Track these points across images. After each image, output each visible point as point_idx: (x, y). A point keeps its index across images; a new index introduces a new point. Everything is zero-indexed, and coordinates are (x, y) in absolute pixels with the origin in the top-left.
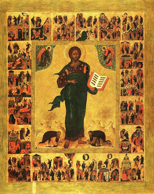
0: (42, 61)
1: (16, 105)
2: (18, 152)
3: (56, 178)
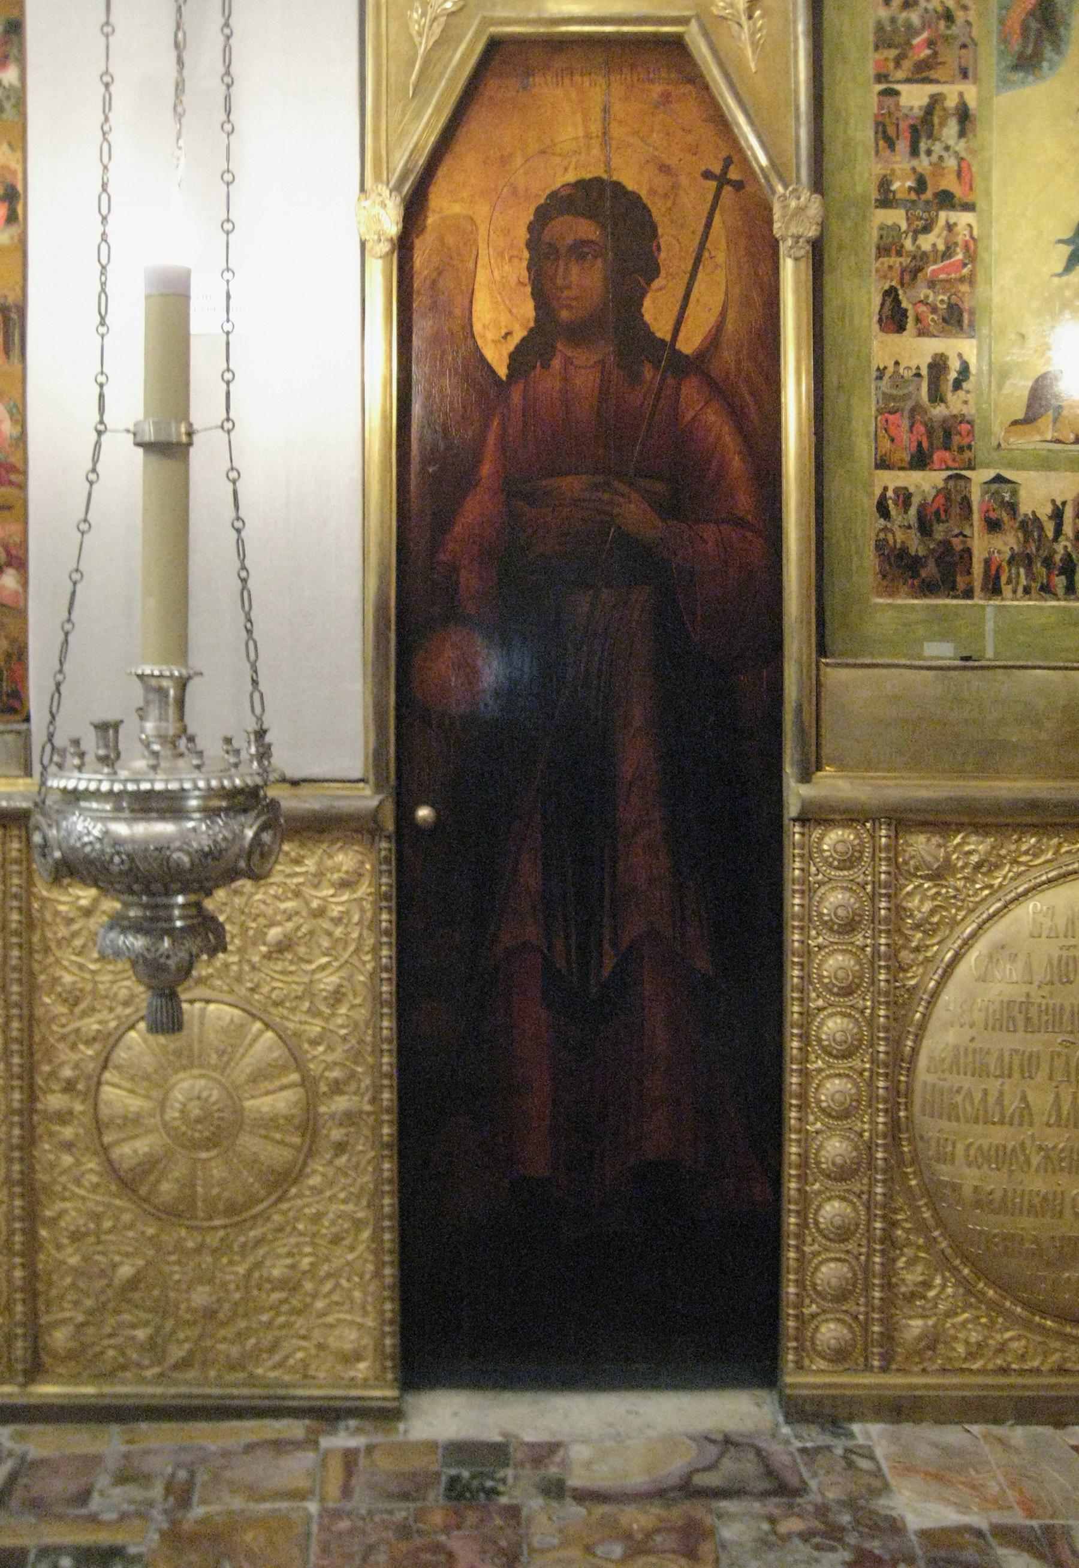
1: (908, 244)
2: (920, 461)
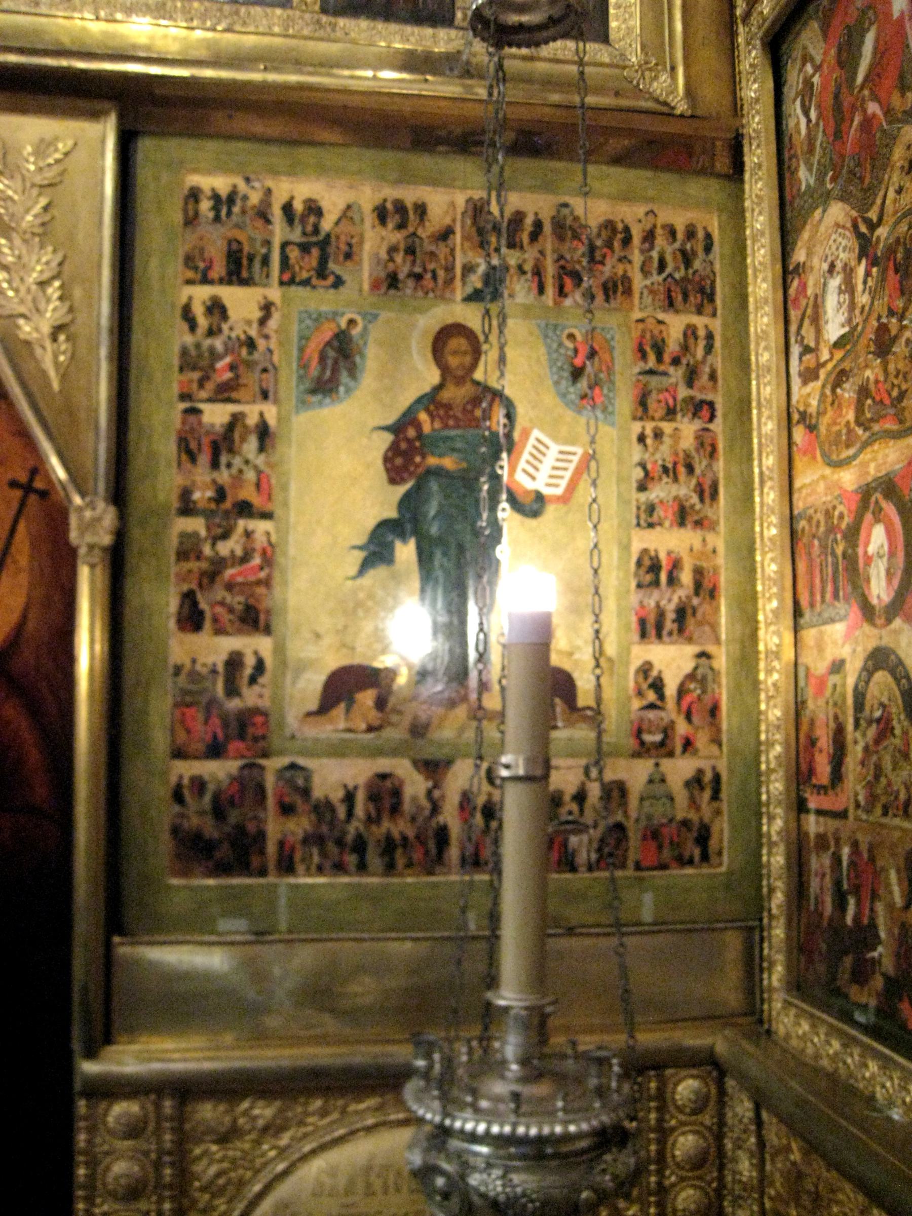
0: (323, 369)
1: (207, 550)
2: (215, 751)
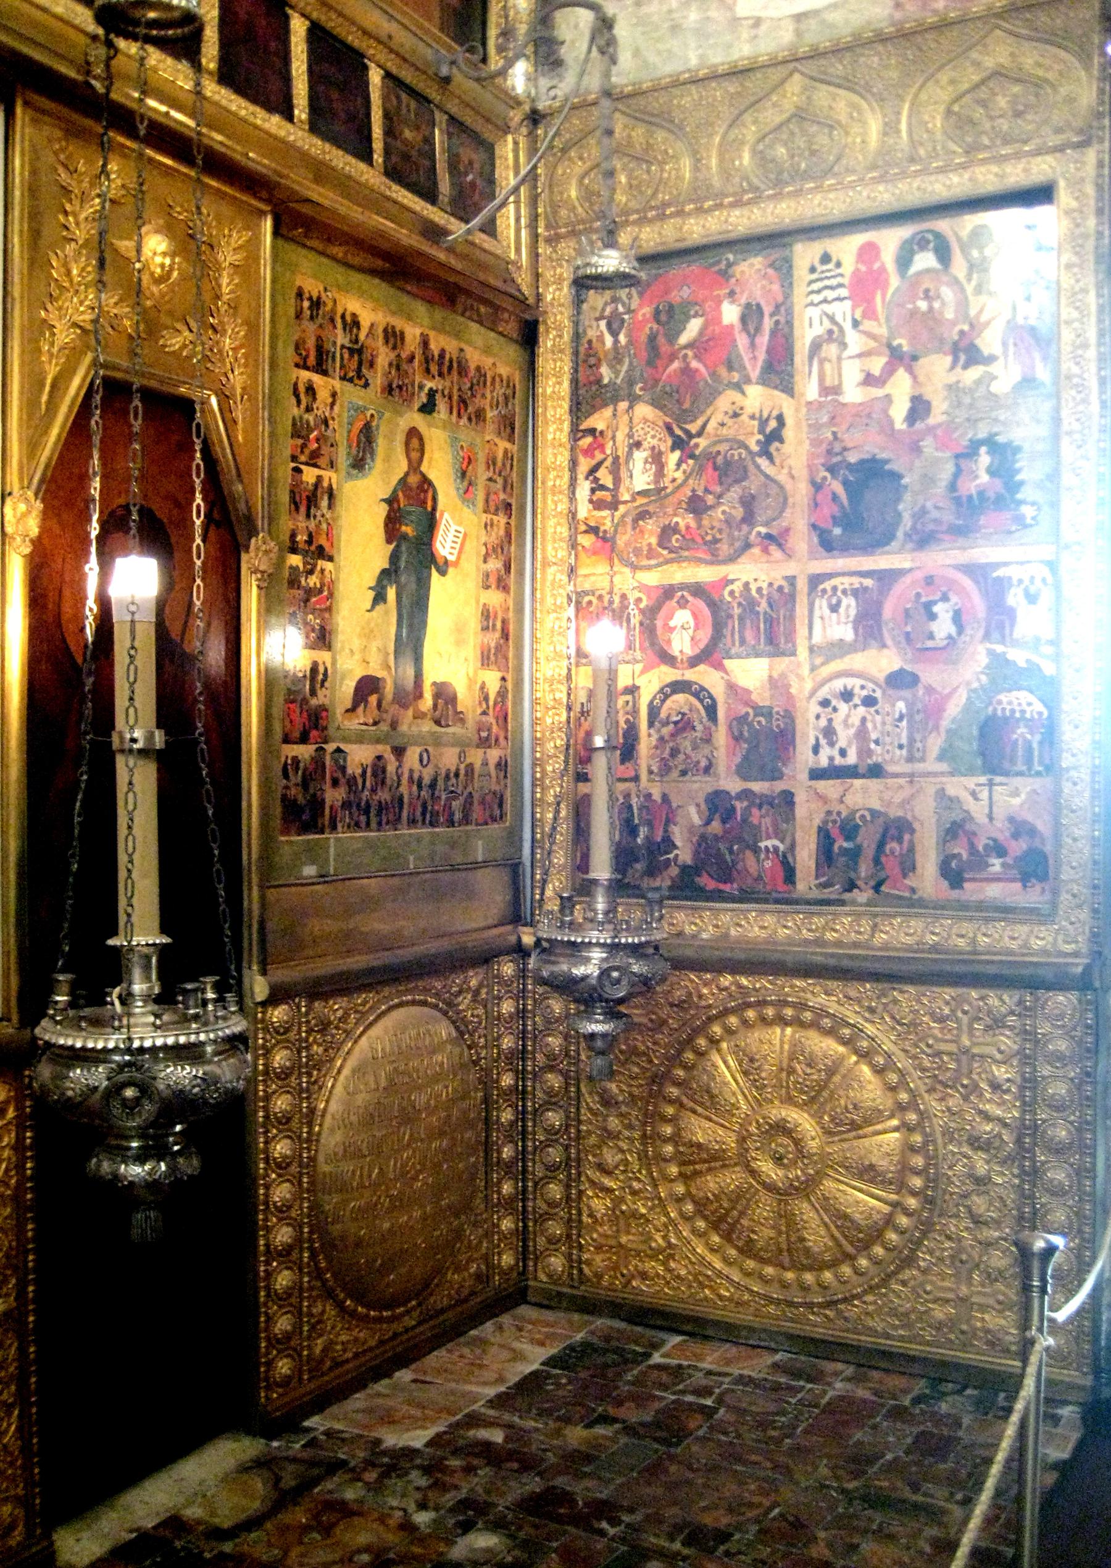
2: (304, 739)
3: (374, 821)
